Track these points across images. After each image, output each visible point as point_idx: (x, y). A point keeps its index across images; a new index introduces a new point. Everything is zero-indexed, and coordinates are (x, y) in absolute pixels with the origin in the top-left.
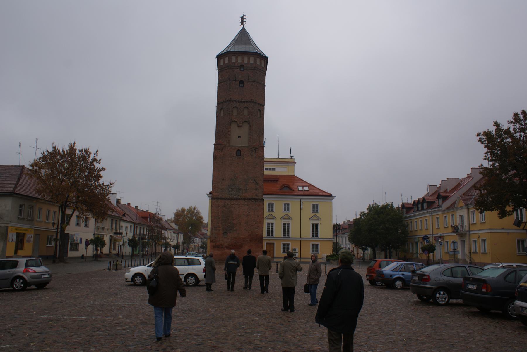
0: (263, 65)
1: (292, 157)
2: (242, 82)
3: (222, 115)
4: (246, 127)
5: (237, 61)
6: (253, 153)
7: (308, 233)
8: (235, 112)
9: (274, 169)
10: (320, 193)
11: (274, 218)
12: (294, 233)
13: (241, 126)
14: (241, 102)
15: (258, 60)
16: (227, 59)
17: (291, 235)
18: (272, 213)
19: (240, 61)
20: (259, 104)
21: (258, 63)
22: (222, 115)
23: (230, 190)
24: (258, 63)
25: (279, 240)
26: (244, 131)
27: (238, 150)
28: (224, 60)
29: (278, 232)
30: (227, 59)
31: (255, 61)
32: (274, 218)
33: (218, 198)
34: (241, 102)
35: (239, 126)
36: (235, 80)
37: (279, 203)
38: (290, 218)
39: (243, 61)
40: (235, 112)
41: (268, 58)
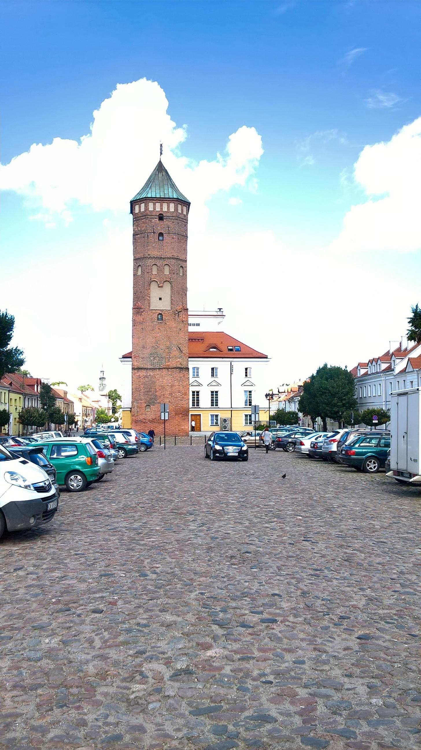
0: (185, 213)
1: (220, 309)
2: (161, 234)
3: (139, 273)
4: (167, 288)
5: (154, 209)
6: (177, 317)
7: (240, 401)
8: (155, 271)
9: (198, 325)
10: (255, 355)
11: (200, 385)
12: (223, 402)
13: (162, 287)
14: (161, 258)
15: (180, 206)
16: (143, 205)
17: (220, 405)
18: (197, 379)
19: (158, 209)
20: (181, 260)
21: (180, 211)
22: (139, 273)
23: (152, 358)
24: (180, 211)
25: (206, 409)
26: (166, 291)
27: (160, 314)
28: (140, 207)
29: (205, 401)
30: (143, 205)
31: (176, 209)
32: (200, 385)
33: (139, 369)
34: (161, 258)
35: (159, 287)
36: (154, 233)
37: (204, 366)
38: (219, 385)
39: (162, 209)
40: (155, 271)
41: (190, 203)
